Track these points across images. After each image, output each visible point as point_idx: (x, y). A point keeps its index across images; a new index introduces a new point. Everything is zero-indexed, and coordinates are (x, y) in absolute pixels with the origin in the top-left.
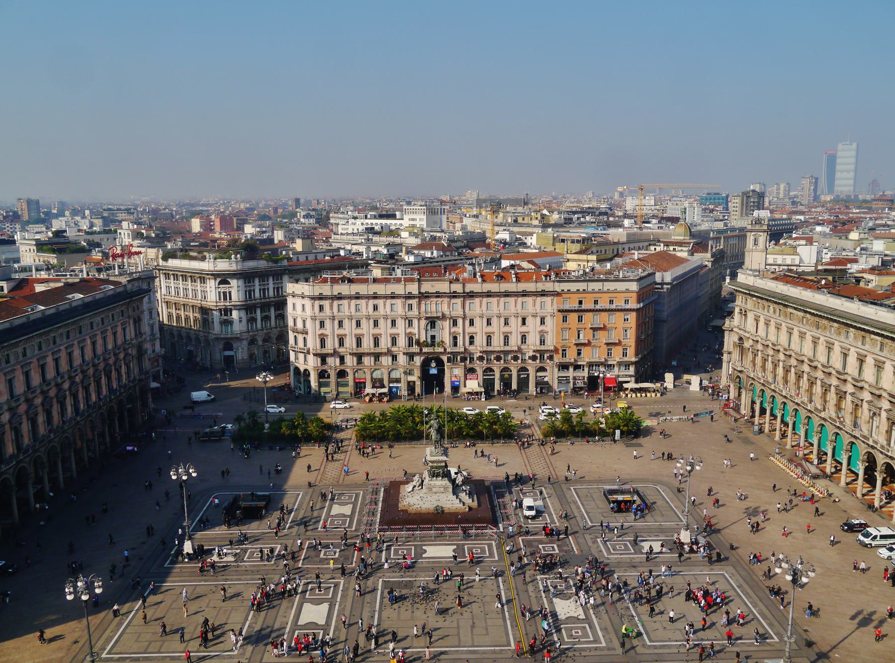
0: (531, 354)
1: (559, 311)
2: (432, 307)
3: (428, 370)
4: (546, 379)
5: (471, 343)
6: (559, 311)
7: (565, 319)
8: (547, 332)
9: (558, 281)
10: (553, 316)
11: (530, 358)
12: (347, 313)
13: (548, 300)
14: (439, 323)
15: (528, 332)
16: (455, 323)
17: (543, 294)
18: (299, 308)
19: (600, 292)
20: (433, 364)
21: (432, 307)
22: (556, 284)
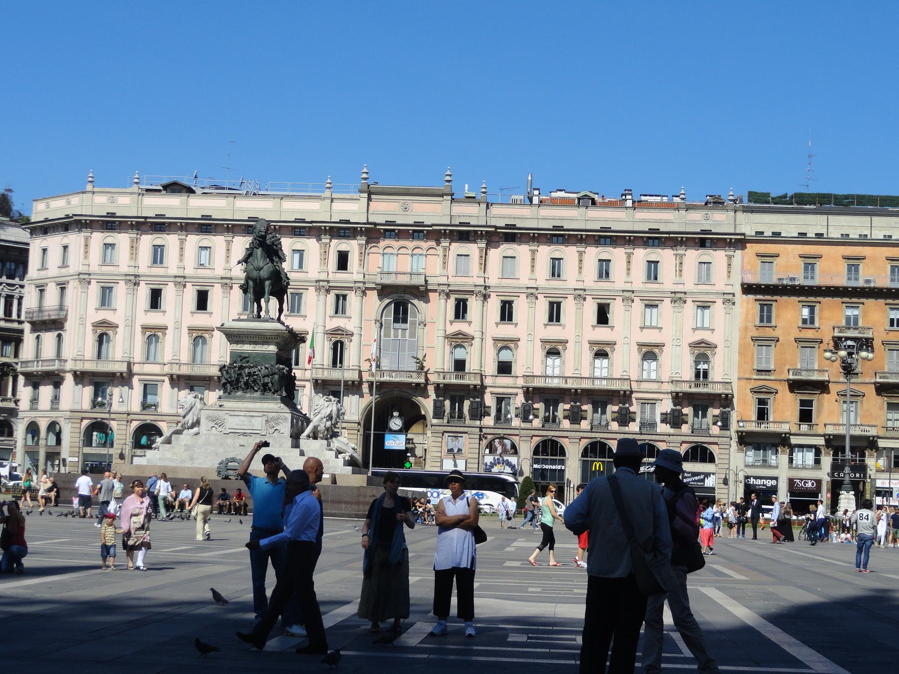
0: (667, 405)
1: (748, 289)
2: (400, 262)
3: (380, 440)
4: (709, 482)
5: (505, 368)
6: (748, 289)
7: (765, 315)
8: (712, 347)
9: (746, 210)
10: (729, 301)
11: (665, 419)
12: (173, 271)
13: (718, 257)
14: (420, 309)
15: (660, 346)
16: (461, 310)
17: (704, 241)
18: (54, 257)
19: (864, 241)
20: (396, 423)
21: (400, 262)
22: (740, 215)
